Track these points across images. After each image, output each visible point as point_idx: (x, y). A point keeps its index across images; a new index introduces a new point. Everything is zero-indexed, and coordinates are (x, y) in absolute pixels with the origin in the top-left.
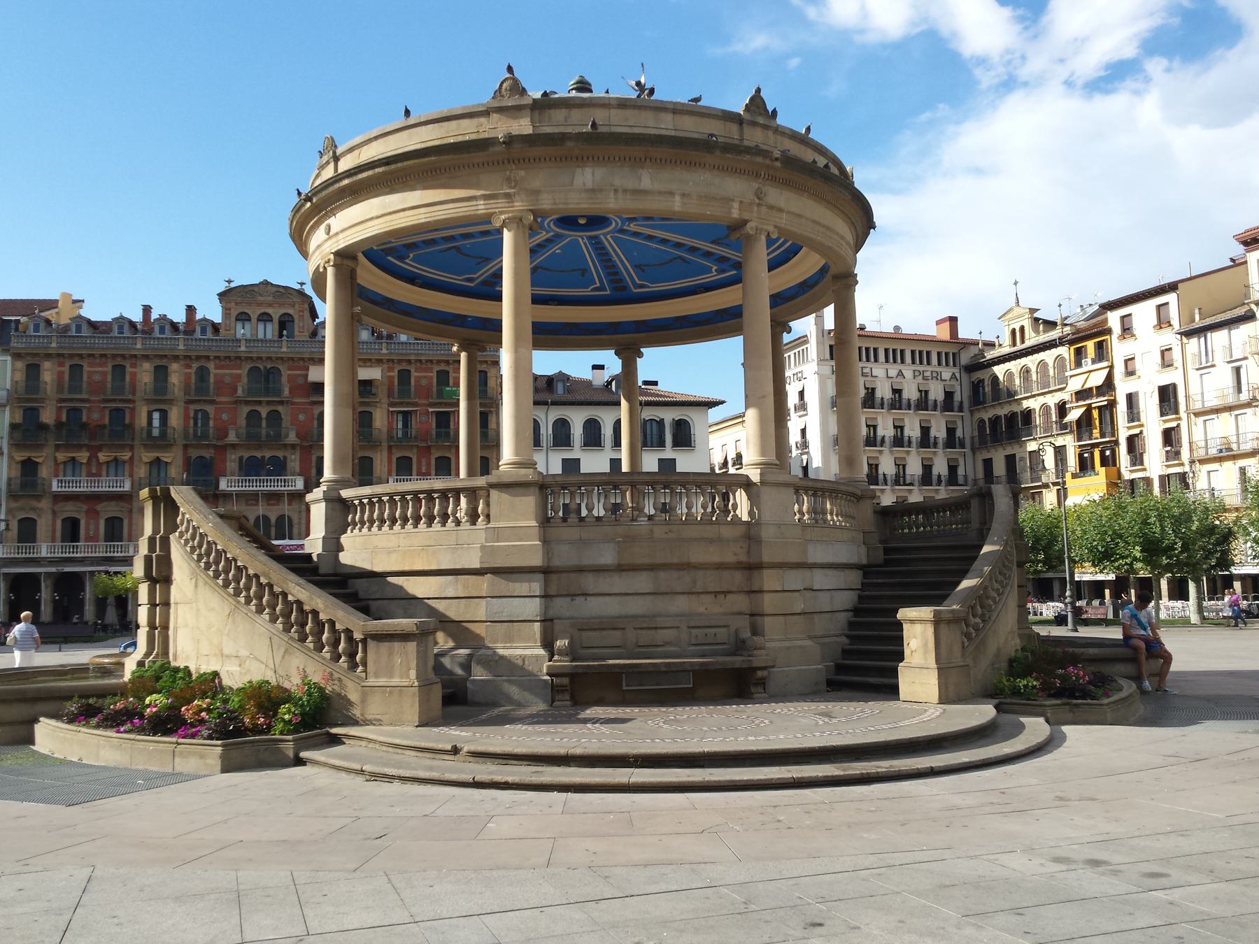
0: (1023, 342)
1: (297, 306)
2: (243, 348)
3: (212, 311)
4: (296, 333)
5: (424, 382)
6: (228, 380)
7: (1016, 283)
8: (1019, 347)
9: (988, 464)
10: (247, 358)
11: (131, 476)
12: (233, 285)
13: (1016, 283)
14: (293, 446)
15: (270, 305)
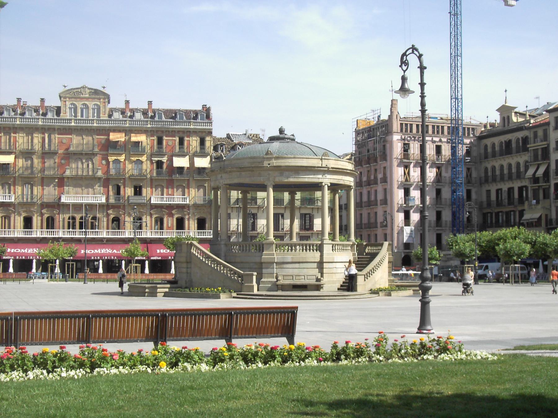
0: (508, 125)
1: (102, 100)
2: (73, 124)
3: (53, 101)
4: (101, 115)
5: (170, 143)
6: (64, 141)
7: (506, 91)
8: (507, 128)
9: (488, 192)
10: (75, 129)
11: (15, 193)
12: (67, 88)
13: (506, 91)
14: (100, 179)
15: (87, 99)
